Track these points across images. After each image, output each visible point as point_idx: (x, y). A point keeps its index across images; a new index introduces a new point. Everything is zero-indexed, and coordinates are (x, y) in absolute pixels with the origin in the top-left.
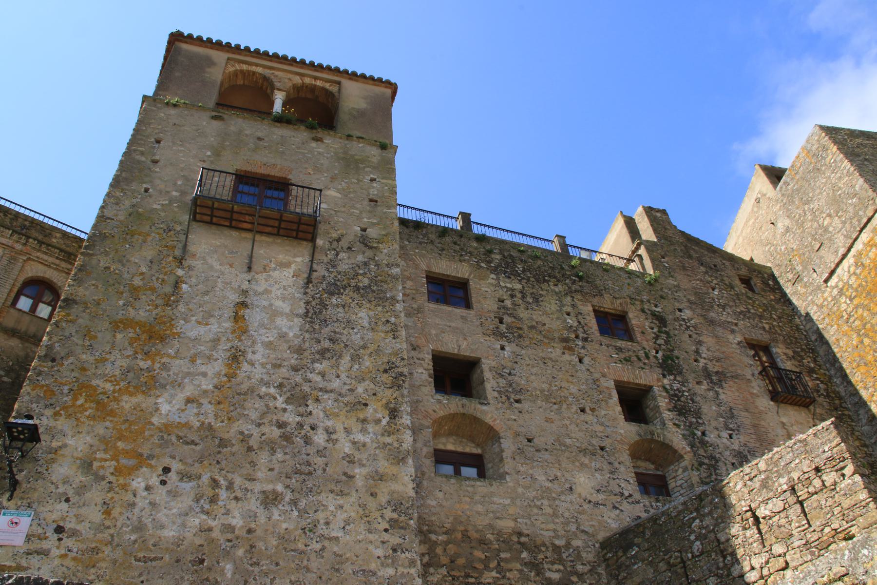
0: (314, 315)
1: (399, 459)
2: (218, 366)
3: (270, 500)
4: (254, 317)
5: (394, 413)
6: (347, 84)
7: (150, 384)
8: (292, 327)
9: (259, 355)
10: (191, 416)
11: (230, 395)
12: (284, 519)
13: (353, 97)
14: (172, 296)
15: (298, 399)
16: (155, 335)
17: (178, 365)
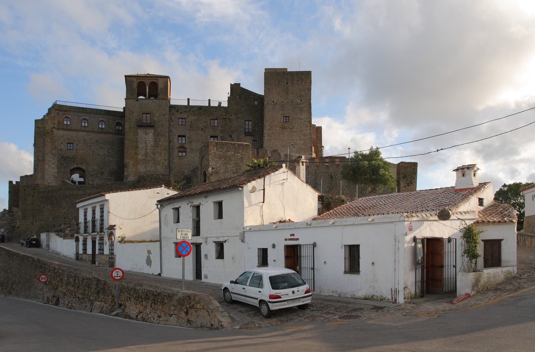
0: (155, 141)
1: (166, 160)
2: (144, 151)
3: (152, 167)
4: (148, 142)
5: (165, 154)
6: (160, 79)
7: (137, 154)
8: (152, 143)
9: (149, 148)
10: (142, 158)
11: (146, 154)
12: (153, 169)
13: (161, 86)
14: (137, 142)
15: (154, 154)
16: (137, 147)
17: (140, 151)
